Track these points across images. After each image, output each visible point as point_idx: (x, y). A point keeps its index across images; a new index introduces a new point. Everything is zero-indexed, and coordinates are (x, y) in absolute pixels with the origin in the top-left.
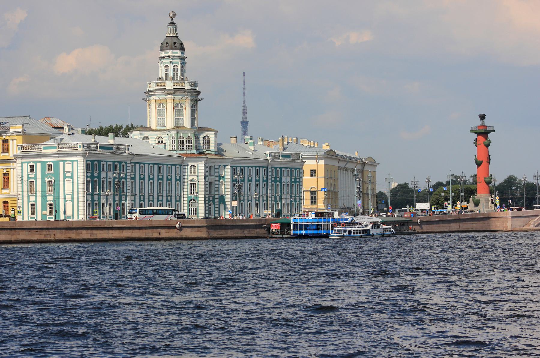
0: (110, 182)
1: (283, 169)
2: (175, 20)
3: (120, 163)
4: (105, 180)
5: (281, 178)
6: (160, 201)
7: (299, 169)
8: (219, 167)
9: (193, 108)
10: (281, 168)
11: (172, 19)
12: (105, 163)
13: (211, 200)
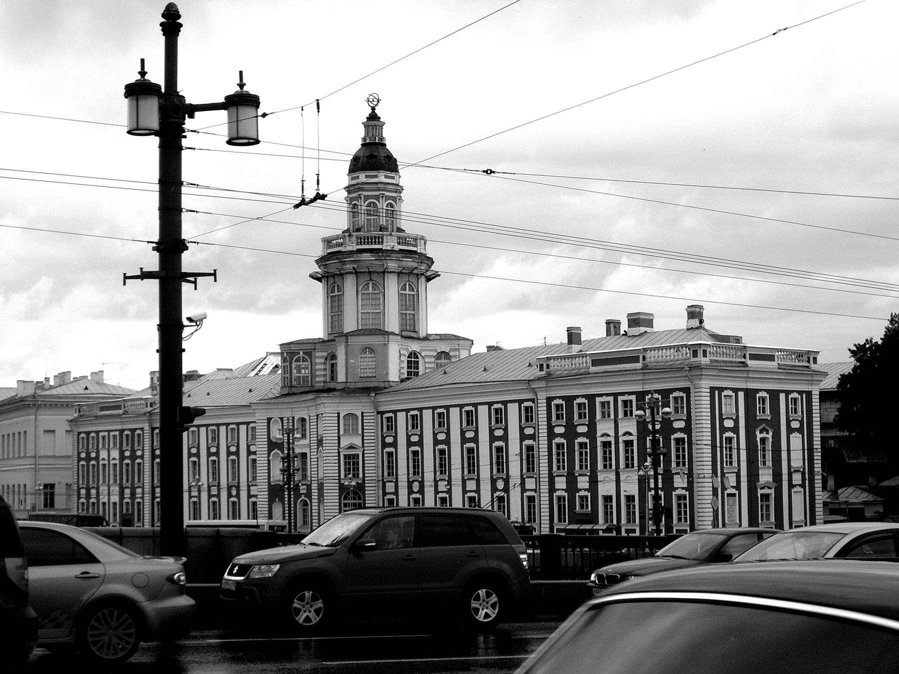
0: (115, 465)
1: (598, 400)
2: (378, 111)
3: (133, 431)
4: (106, 462)
5: (592, 426)
6: (214, 496)
7: (687, 390)
8: (317, 418)
9: (336, 293)
10: (591, 398)
11: (373, 109)
12: (106, 434)
13: (303, 494)
